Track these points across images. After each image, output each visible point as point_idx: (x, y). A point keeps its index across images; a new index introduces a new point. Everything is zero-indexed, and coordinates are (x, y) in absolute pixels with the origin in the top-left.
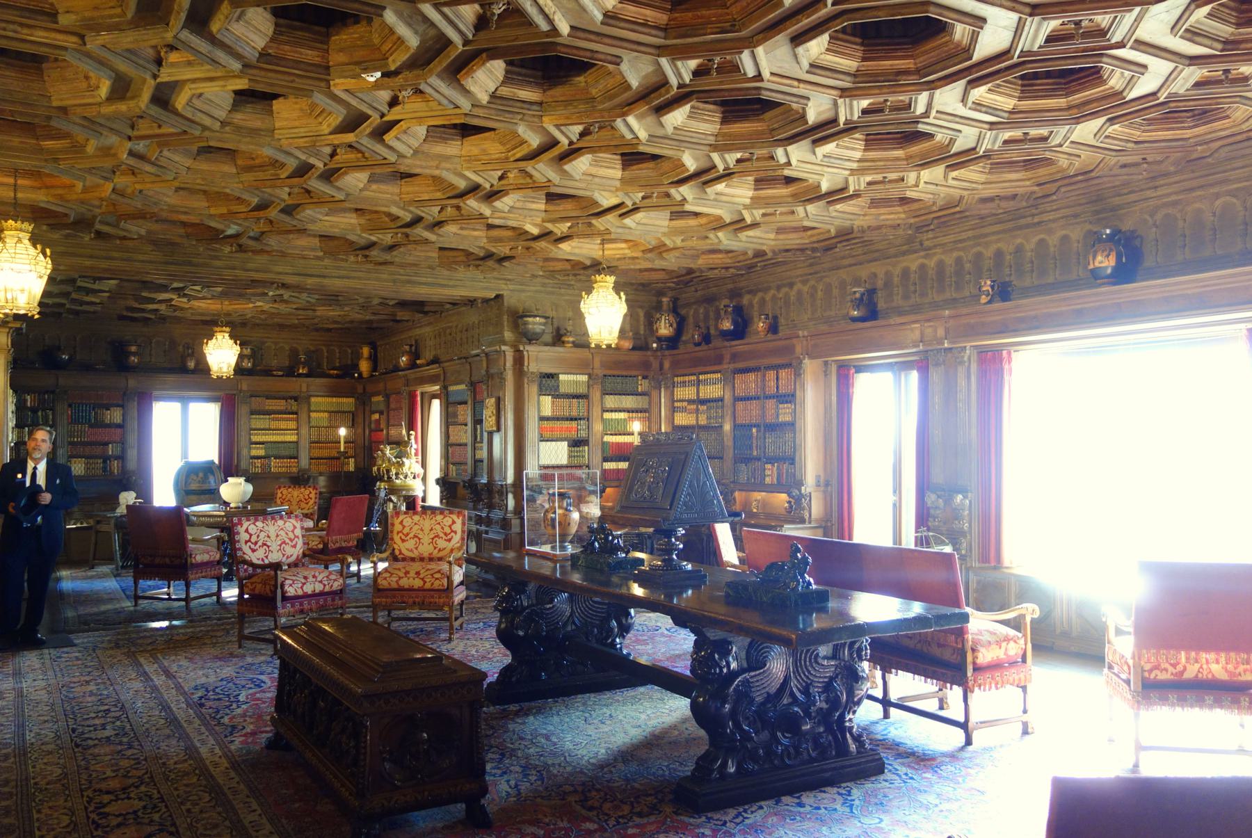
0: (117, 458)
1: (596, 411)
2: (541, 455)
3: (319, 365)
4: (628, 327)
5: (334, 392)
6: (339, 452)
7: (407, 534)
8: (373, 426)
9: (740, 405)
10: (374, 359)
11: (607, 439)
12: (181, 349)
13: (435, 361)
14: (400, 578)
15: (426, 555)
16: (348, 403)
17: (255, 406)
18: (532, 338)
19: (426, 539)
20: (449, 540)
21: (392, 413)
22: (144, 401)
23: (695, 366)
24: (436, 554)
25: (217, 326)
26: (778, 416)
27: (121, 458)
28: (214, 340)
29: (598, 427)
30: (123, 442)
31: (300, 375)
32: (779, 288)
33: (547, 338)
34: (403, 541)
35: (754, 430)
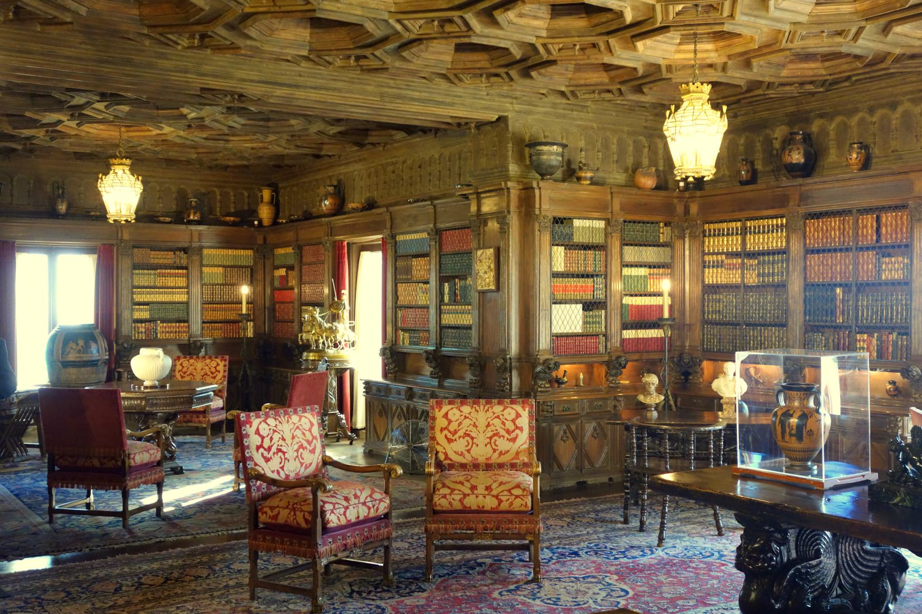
1: (615, 264)
2: (554, 323)
3: (211, 211)
4: (726, 154)
5: (228, 243)
6: (241, 315)
7: (456, 432)
8: (277, 284)
9: (814, 260)
10: (275, 203)
11: (628, 300)
12: (48, 188)
13: (371, 205)
14: (465, 495)
15: (481, 460)
16: (245, 255)
18: (544, 172)
19: (481, 439)
20: (514, 440)
21: (305, 268)
23: (741, 210)
24: (495, 458)
25: (115, 157)
26: (879, 273)
28: (111, 175)
29: (617, 286)
31: (190, 222)
32: (871, 110)
33: (559, 174)
34: (450, 441)
35: (838, 290)
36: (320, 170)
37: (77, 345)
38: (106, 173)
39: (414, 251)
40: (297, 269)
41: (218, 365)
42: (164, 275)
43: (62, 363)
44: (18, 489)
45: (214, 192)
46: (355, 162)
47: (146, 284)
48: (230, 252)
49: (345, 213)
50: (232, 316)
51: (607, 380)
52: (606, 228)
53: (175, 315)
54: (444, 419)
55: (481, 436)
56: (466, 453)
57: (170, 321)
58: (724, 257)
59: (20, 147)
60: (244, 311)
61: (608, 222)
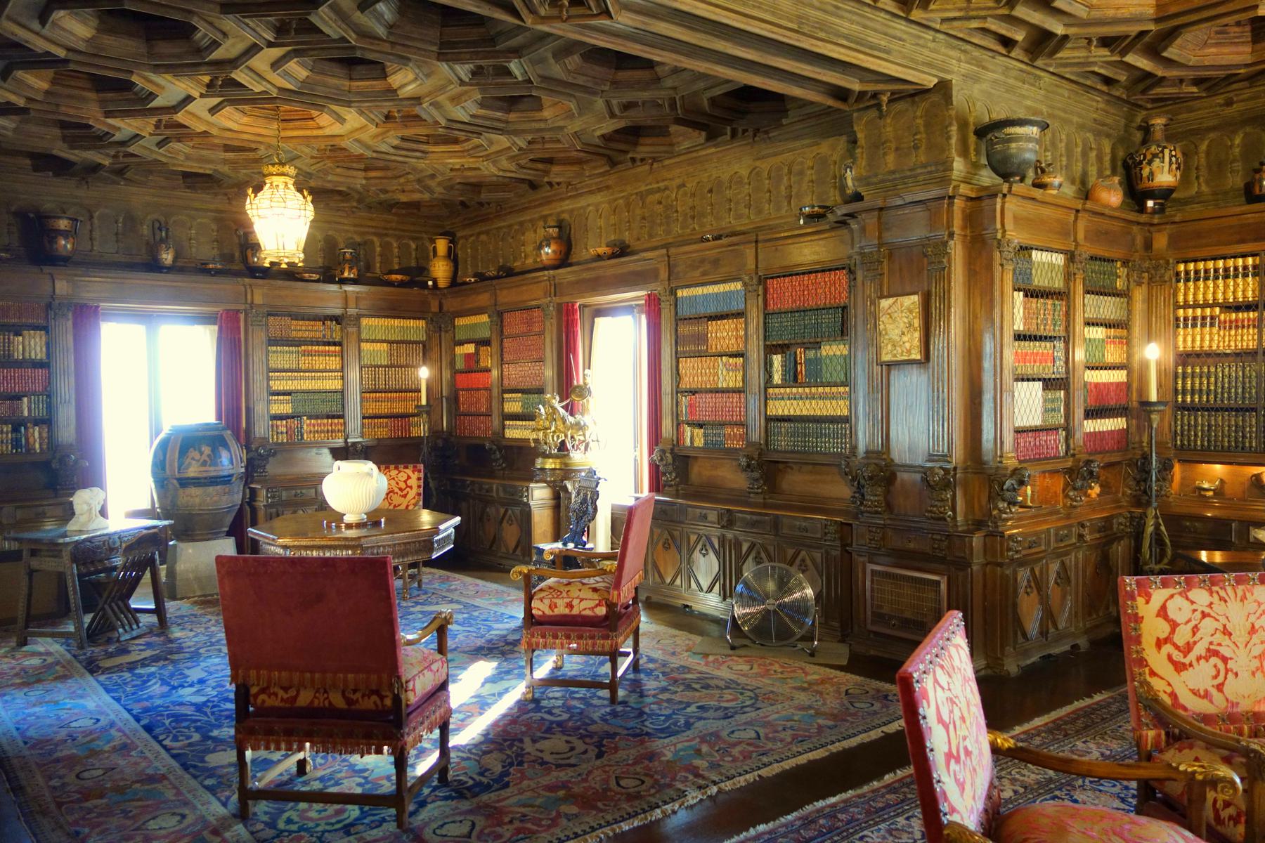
0: (37, 422)
3: (369, 267)
5: (392, 310)
7: (1188, 648)
8: (460, 365)
10: (452, 256)
12: (145, 230)
17: (275, 332)
22: (85, 316)
27: (47, 422)
29: (1080, 355)
30: (48, 394)
31: (343, 281)
34: (1179, 667)
36: (527, 208)
37: (201, 453)
38: (258, 189)
39: (712, 310)
40: (495, 344)
41: (409, 477)
42: (310, 354)
43: (179, 480)
44: (146, 710)
45: (372, 242)
46: (591, 192)
47: (286, 367)
48: (397, 322)
49: (571, 265)
50: (399, 408)
51: (1067, 496)
52: (1067, 266)
53: (325, 409)
54: (1161, 620)
55: (1242, 652)
56: (1214, 692)
57: (317, 417)
58: (1217, 310)
59: (107, 162)
60: (424, 402)
61: (1071, 257)
